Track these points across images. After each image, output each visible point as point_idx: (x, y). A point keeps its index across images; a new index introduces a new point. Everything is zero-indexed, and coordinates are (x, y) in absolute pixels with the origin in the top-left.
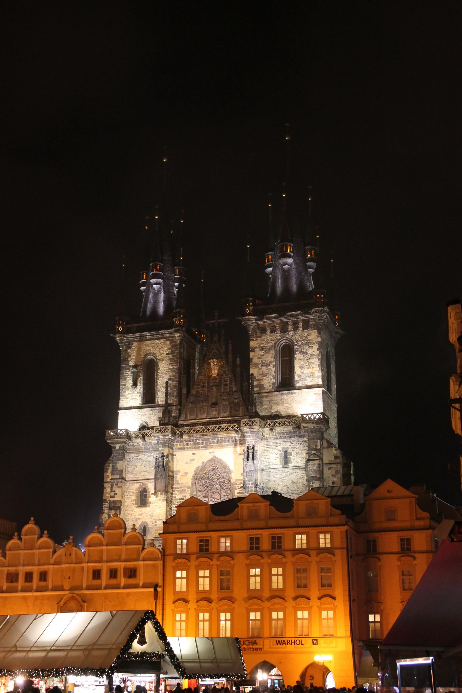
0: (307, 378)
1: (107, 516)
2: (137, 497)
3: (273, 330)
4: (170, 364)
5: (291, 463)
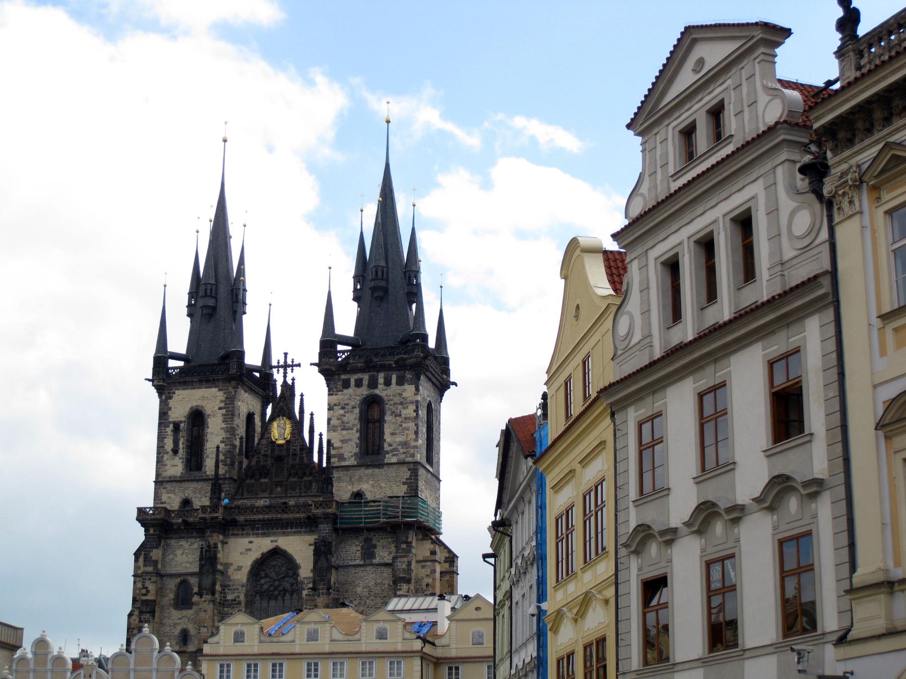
1: (137, 620)
2: (177, 596)
3: (359, 384)
5: (375, 558)
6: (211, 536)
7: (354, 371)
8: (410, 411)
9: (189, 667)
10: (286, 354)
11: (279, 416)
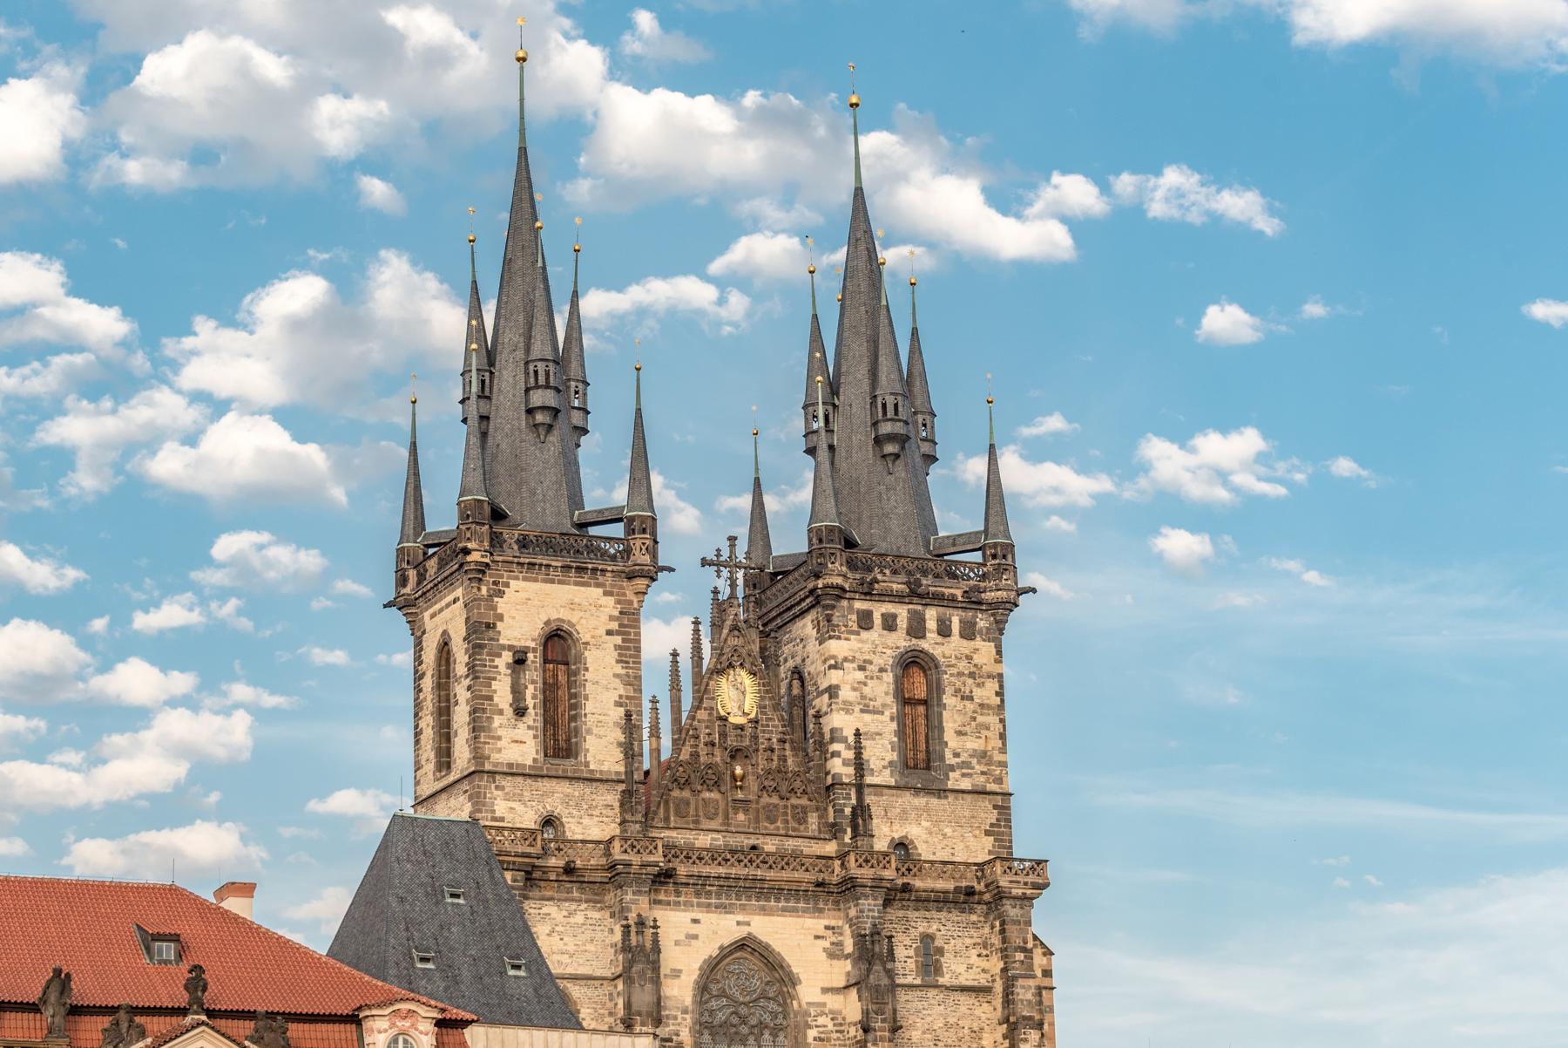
0: (974, 761)
3: (889, 624)
4: (618, 662)
6: (634, 902)
8: (987, 693)
10: (732, 539)
11: (731, 666)
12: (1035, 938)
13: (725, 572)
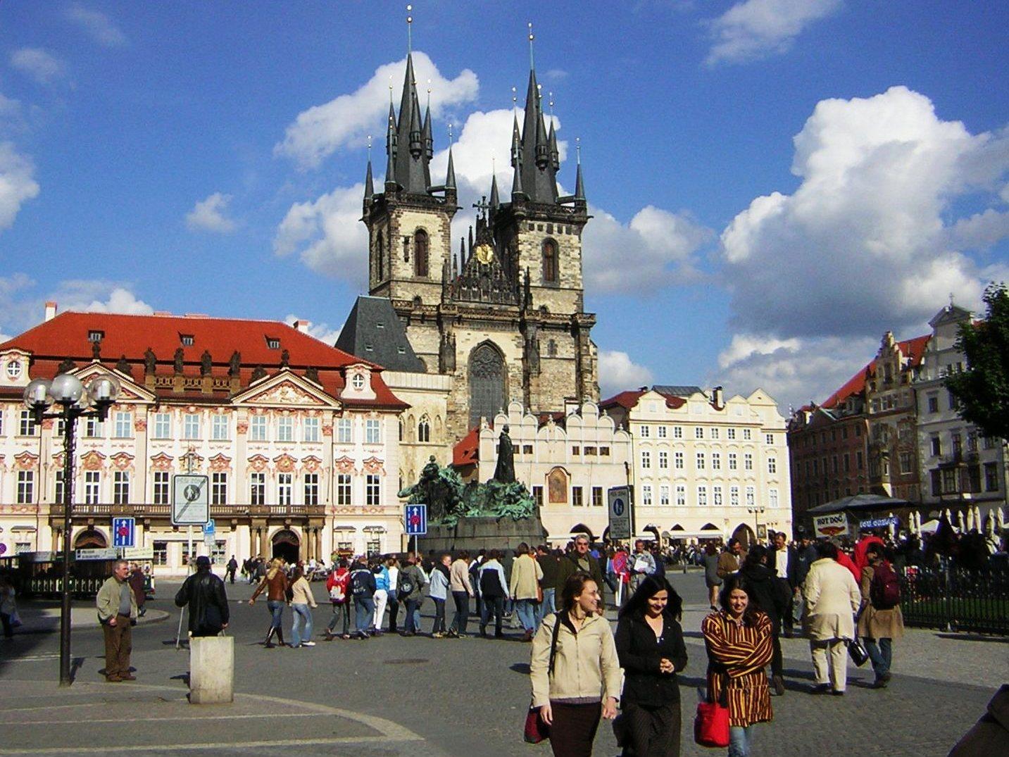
3: (540, 228)
7: (539, 219)
8: (575, 254)
9: (621, 428)
10: (484, 198)
11: (483, 243)
12: (591, 341)
13: (481, 209)
